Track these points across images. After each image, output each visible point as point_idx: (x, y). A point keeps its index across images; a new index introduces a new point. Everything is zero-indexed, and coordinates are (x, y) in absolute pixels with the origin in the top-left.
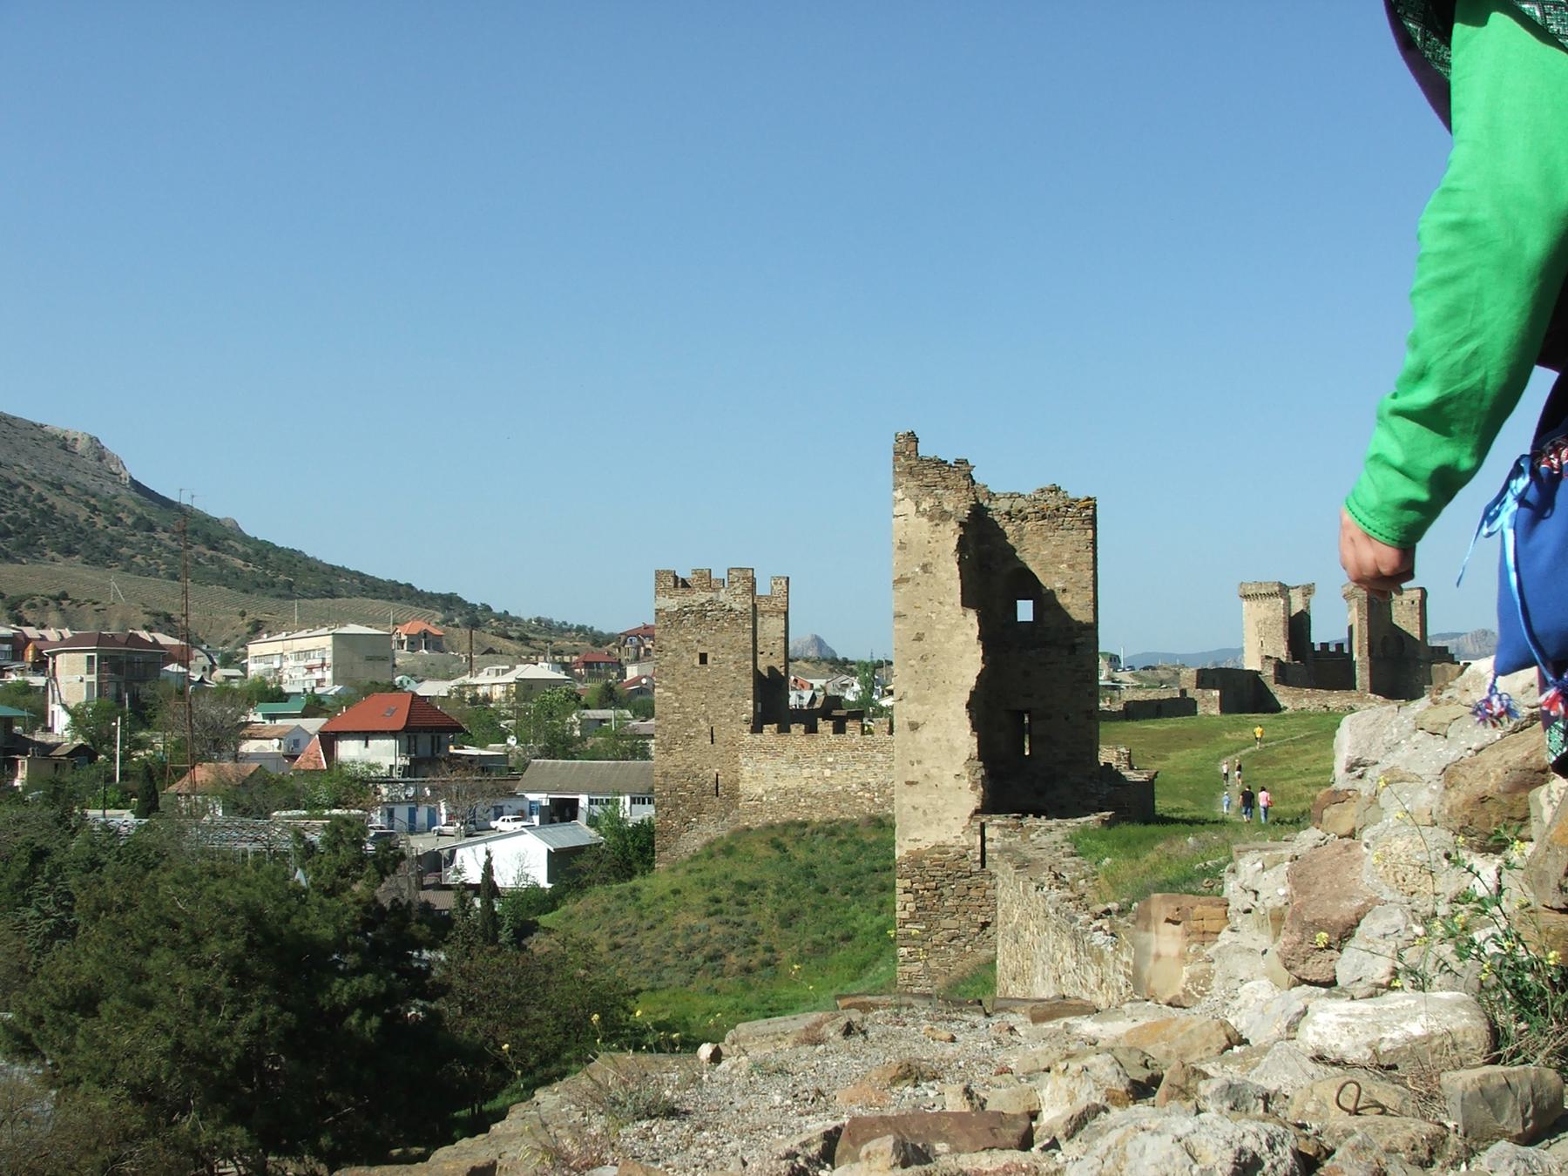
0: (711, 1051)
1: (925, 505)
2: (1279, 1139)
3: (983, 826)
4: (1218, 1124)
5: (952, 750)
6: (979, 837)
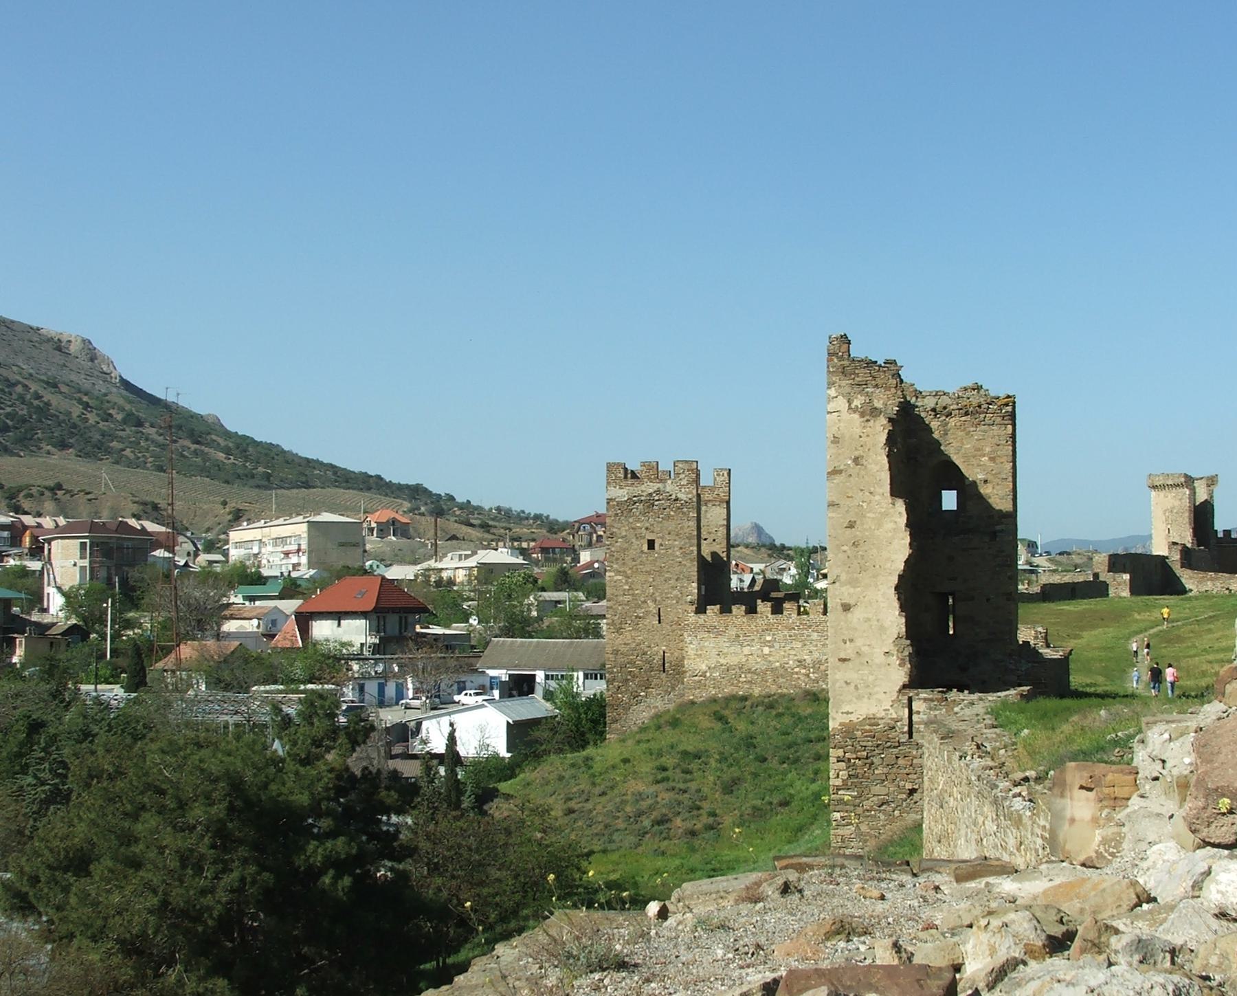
0: (658, 909)
1: (857, 403)
2: (1184, 990)
3: (910, 700)
4: (1128, 976)
5: (882, 629)
6: (906, 710)
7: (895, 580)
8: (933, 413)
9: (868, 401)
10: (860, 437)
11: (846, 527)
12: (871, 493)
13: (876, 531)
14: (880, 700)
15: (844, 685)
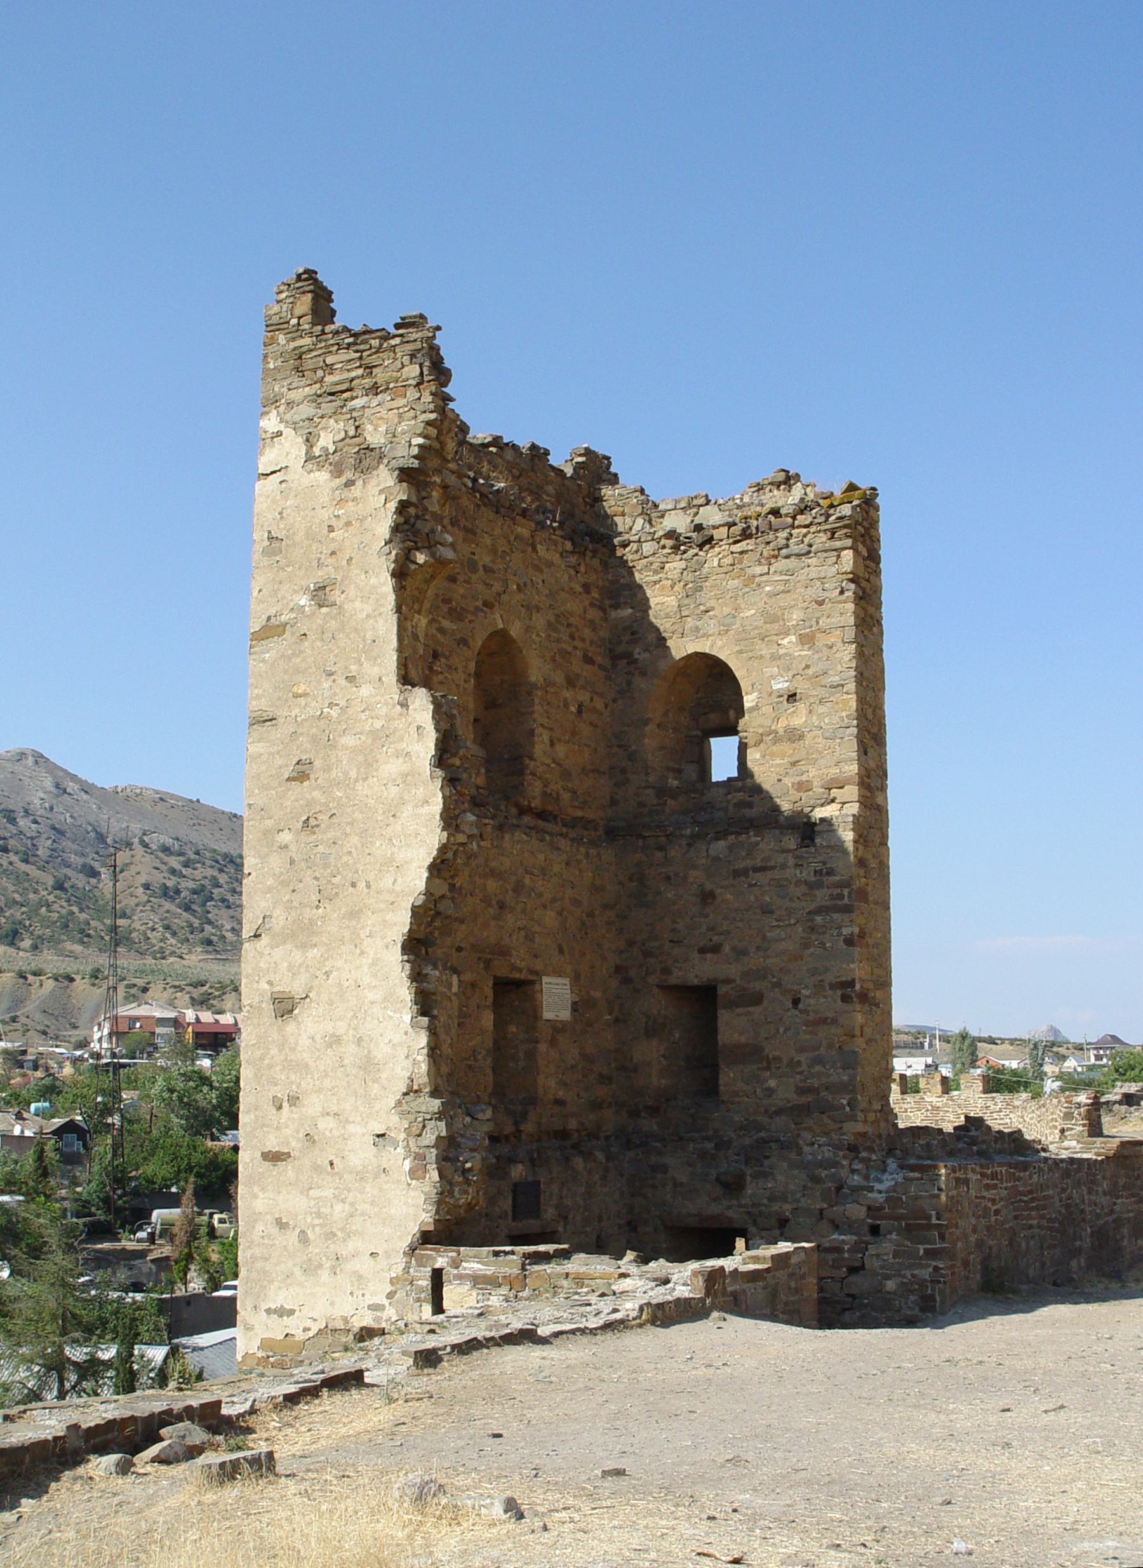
1: (326, 441)
3: (437, 1277)
5: (369, 1066)
7: (401, 923)
8: (669, 543)
9: (352, 433)
10: (331, 529)
11: (288, 779)
12: (351, 679)
13: (359, 786)
14: (360, 1277)
15: (274, 1230)
